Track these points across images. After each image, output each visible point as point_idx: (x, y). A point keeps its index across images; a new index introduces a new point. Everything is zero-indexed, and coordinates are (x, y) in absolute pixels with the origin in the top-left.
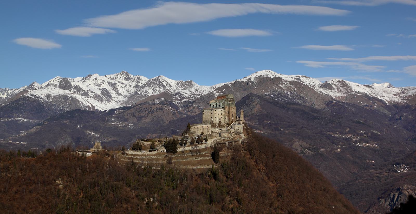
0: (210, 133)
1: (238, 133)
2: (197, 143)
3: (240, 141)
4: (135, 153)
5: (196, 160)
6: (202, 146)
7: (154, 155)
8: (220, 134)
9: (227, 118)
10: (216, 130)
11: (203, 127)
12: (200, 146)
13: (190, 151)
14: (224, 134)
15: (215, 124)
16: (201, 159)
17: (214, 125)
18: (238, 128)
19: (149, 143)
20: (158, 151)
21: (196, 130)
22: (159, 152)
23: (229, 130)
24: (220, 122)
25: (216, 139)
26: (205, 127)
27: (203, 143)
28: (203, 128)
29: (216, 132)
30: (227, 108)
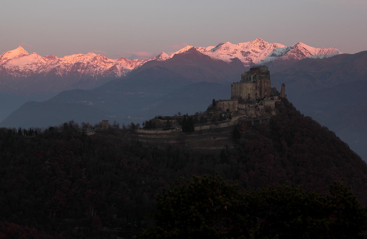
0: (236, 110)
1: (268, 110)
2: (219, 121)
3: (269, 120)
4: (147, 132)
5: (214, 139)
6: (223, 125)
7: (167, 134)
8: (246, 111)
9: (258, 93)
10: (244, 106)
11: (228, 103)
12: (222, 124)
13: (210, 130)
14: (250, 111)
15: (244, 100)
16: (221, 139)
17: (241, 101)
18: (268, 105)
19: (166, 121)
20: (172, 130)
21: (222, 107)
22: (174, 130)
23: (256, 107)
24: (249, 97)
25: (241, 116)
26: (231, 103)
27: (226, 121)
28: (229, 105)
29: (243, 109)
30: (259, 81)
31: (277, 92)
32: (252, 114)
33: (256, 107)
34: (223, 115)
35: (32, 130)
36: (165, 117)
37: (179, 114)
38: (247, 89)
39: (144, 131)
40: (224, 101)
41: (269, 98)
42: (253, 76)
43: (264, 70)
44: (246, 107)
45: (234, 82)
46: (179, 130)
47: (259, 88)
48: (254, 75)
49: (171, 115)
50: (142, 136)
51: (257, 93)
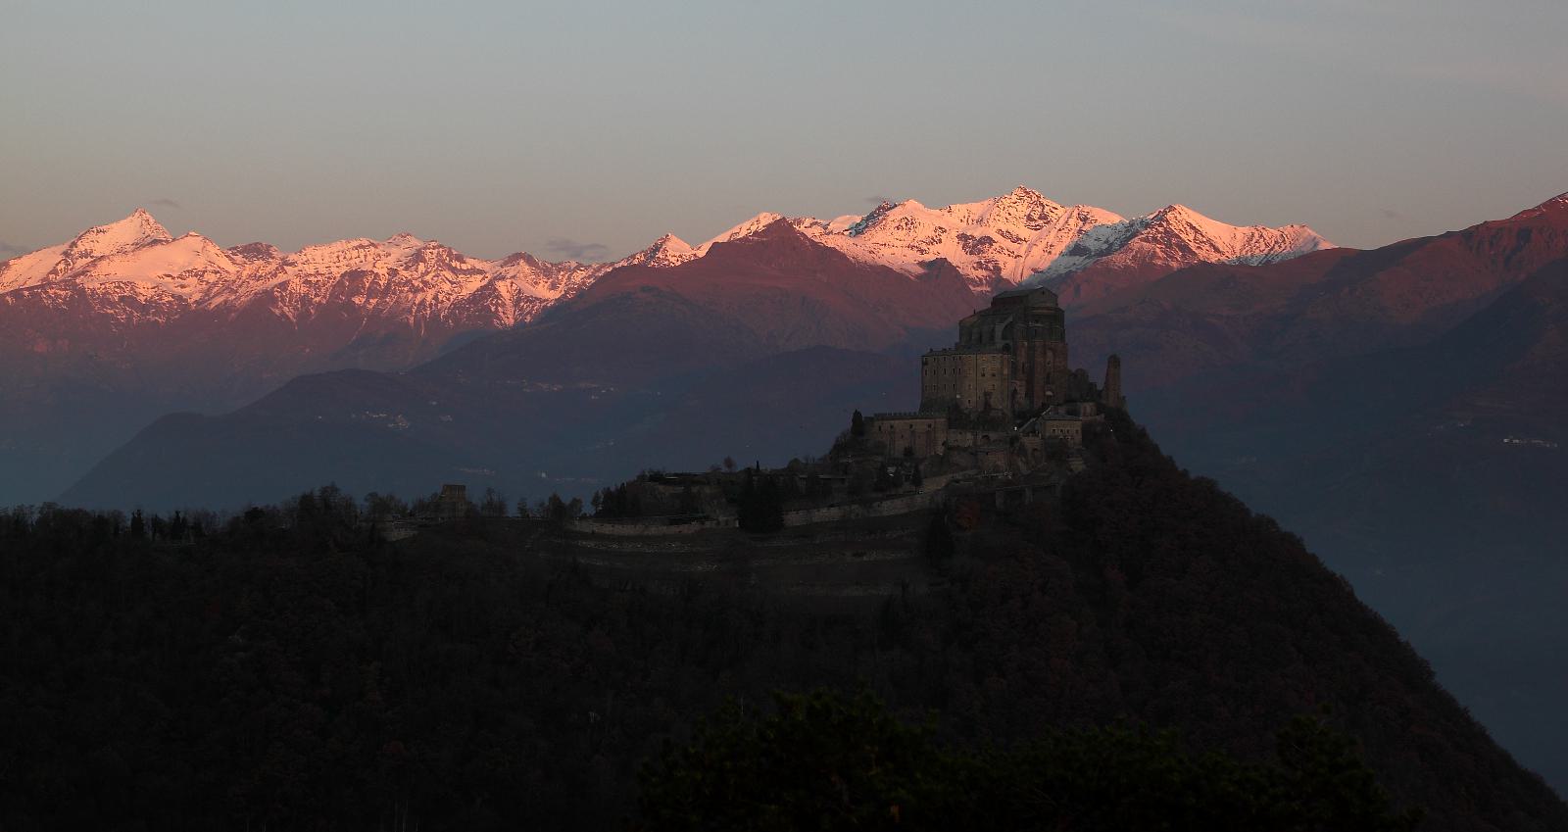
0: (940, 450)
1: (1057, 451)
4: (607, 529)
6: (890, 508)
8: (974, 454)
9: (1022, 392)
10: (967, 439)
11: (911, 426)
12: (886, 504)
19: (680, 489)
22: (708, 524)
23: (1014, 440)
24: (987, 405)
25: (958, 476)
26: (920, 425)
27: (901, 491)
28: (913, 432)
29: (965, 450)
30: (1023, 345)
31: (1092, 386)
32: (997, 469)
33: (1014, 440)
34: (891, 470)
35: (184, 519)
36: (676, 475)
37: (729, 463)
38: (979, 375)
39: (596, 528)
40: (893, 419)
41: (1062, 410)
42: (1004, 325)
43: (1043, 305)
44: (975, 443)
45: (931, 350)
46: (727, 522)
47: (1023, 372)
48: (1006, 323)
49: (699, 467)
50: (591, 544)
51: (1018, 389)
